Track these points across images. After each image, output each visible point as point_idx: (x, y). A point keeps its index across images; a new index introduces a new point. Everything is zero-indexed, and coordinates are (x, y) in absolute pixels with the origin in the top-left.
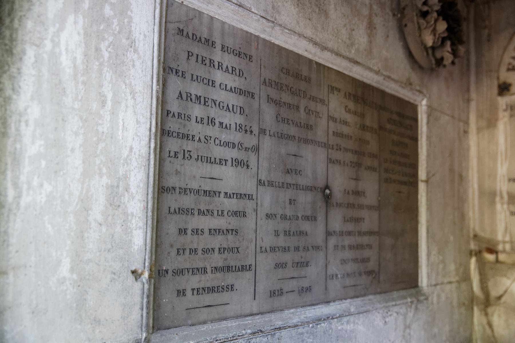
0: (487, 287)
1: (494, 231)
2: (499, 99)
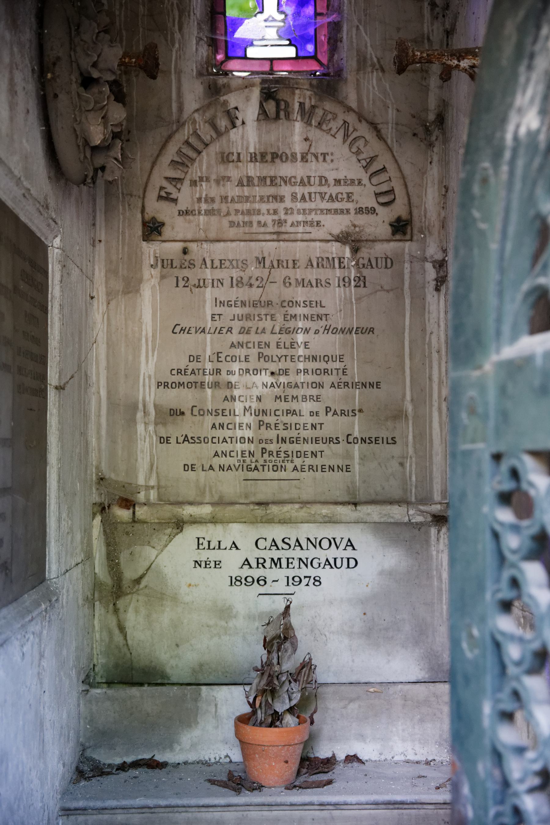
0: (118, 564)
1: (132, 470)
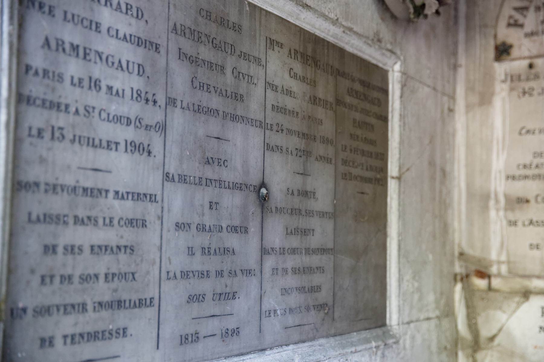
0: (476, 324)
1: (486, 247)
2: (496, 65)
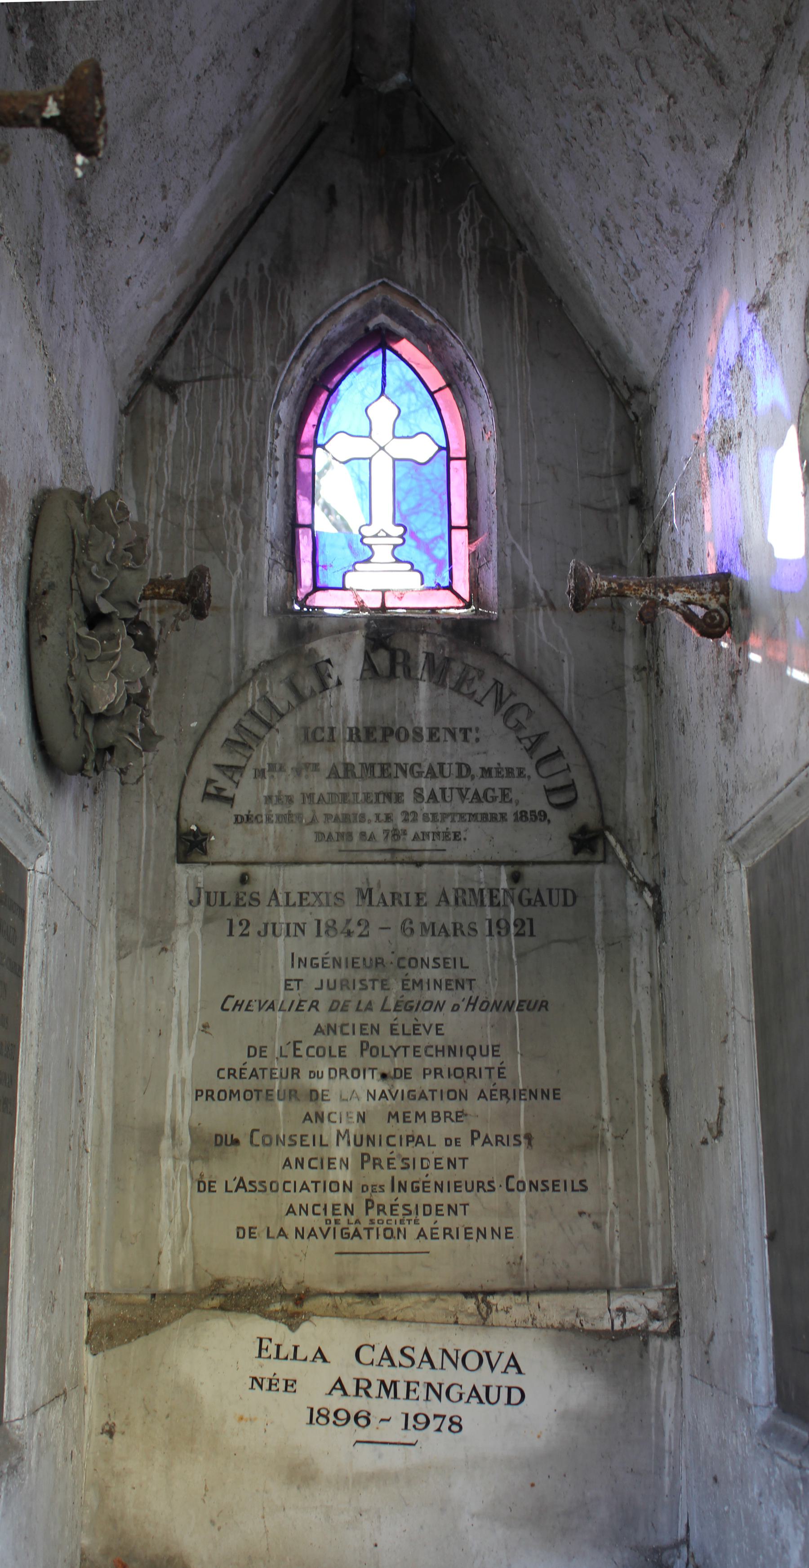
2: (179, 868)
